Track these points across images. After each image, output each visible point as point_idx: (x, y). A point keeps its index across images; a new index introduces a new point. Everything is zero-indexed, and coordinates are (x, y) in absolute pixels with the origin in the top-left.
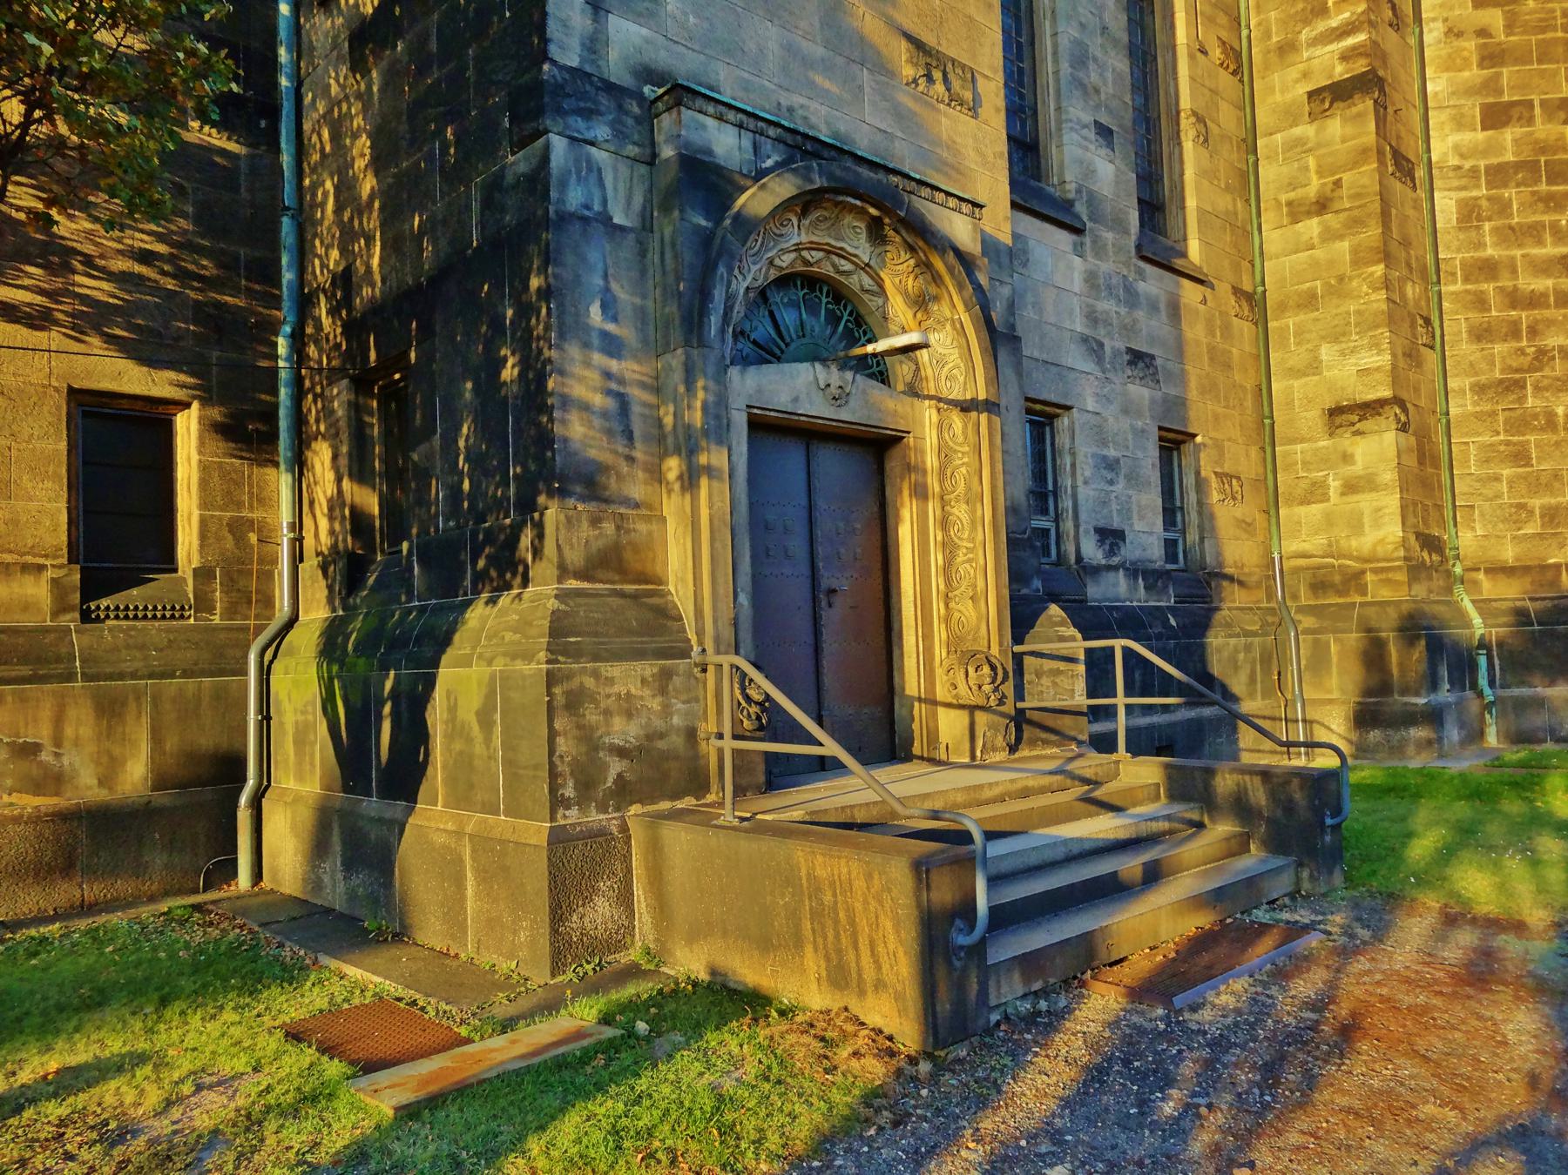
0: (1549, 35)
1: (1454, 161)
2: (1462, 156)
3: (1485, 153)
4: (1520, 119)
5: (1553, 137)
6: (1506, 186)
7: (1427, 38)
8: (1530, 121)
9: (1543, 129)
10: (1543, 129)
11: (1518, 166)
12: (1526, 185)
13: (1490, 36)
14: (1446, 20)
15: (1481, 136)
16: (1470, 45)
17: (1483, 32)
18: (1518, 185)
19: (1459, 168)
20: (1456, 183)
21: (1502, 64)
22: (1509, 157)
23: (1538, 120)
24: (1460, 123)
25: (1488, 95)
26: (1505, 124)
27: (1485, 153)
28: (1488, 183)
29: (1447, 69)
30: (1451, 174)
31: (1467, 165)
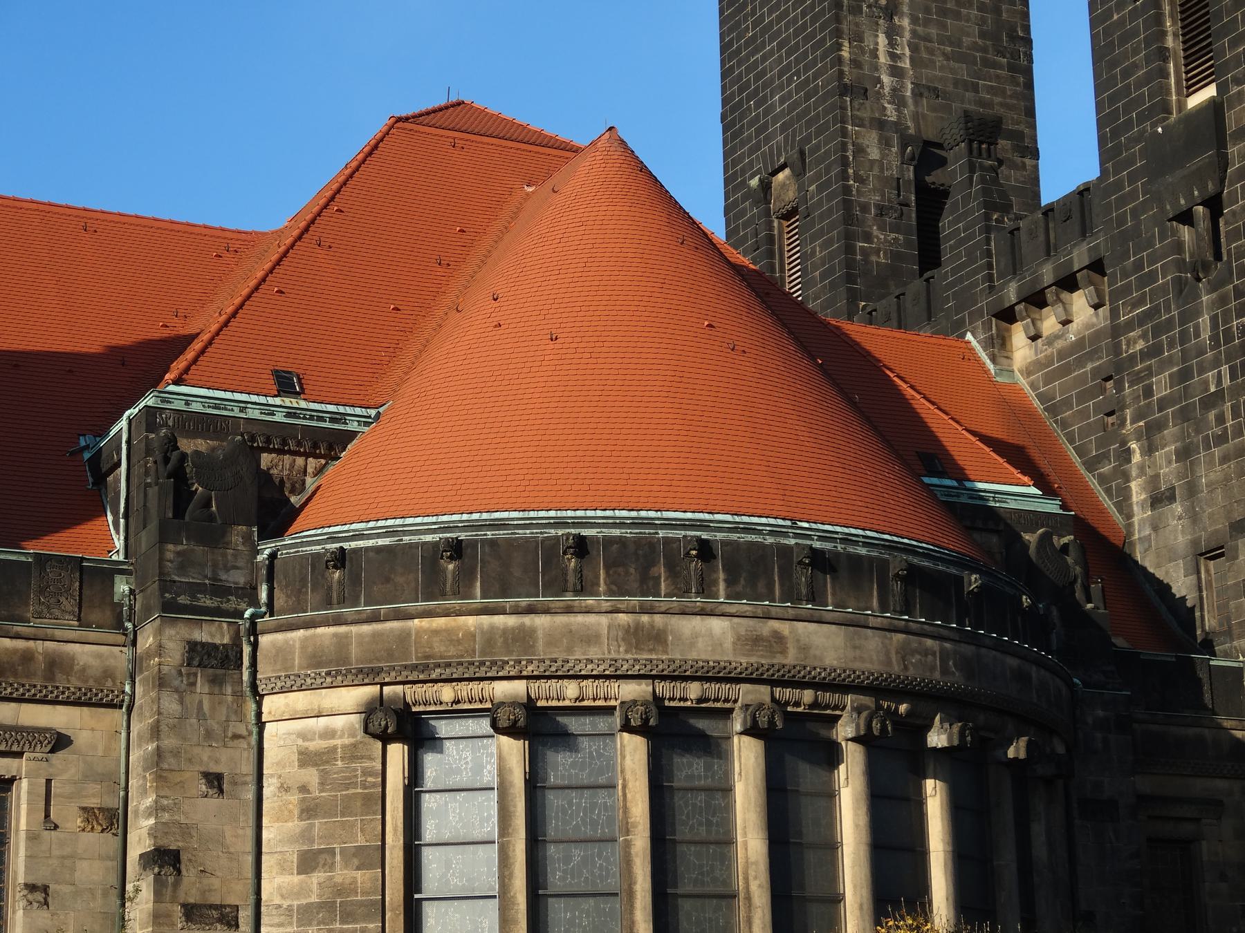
0: (352, 791)
1: (277, 901)
2: (282, 896)
3: (298, 895)
4: (325, 864)
5: (347, 882)
6: (310, 925)
7: (266, 792)
8: (332, 867)
9: (343, 874)
10: (343, 874)
11: (321, 906)
12: (324, 924)
13: (308, 792)
14: (280, 777)
15: (296, 879)
16: (294, 798)
17: (303, 789)
18: (318, 924)
19: (280, 906)
20: (276, 920)
21: (316, 816)
22: (314, 899)
23: (338, 866)
24: (283, 869)
25: (303, 844)
26: (313, 869)
27: (298, 895)
28: (299, 920)
29: (278, 820)
30: (274, 912)
31: (285, 904)
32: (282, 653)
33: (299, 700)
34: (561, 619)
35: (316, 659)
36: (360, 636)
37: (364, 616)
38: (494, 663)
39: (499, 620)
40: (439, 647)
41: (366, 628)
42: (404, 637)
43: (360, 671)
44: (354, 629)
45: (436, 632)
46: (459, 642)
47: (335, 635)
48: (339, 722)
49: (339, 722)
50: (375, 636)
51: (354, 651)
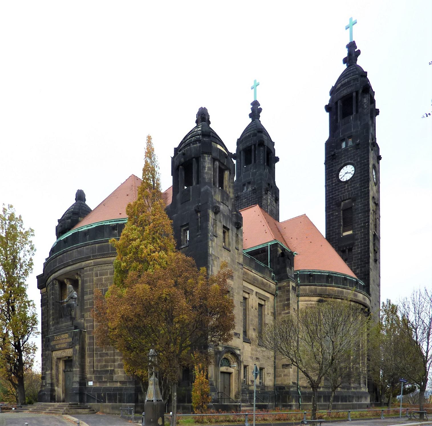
32: (305, 290)
33: (307, 298)
34: (347, 290)
35: (311, 291)
36: (319, 288)
37: (320, 285)
38: (338, 296)
39: (339, 289)
40: (331, 292)
41: (320, 287)
42: (326, 289)
43: (319, 294)
44: (318, 287)
45: (331, 289)
46: (334, 291)
47: (314, 288)
48: (313, 303)
49: (313, 303)
50: (322, 289)
51: (318, 291)
